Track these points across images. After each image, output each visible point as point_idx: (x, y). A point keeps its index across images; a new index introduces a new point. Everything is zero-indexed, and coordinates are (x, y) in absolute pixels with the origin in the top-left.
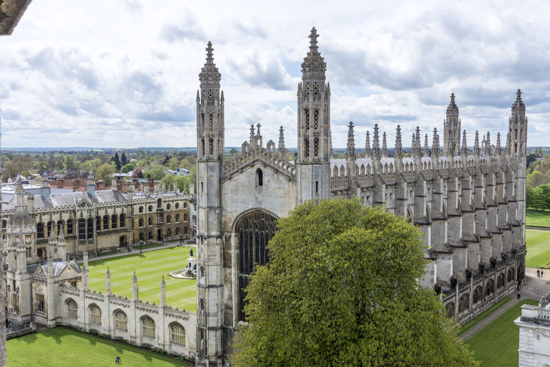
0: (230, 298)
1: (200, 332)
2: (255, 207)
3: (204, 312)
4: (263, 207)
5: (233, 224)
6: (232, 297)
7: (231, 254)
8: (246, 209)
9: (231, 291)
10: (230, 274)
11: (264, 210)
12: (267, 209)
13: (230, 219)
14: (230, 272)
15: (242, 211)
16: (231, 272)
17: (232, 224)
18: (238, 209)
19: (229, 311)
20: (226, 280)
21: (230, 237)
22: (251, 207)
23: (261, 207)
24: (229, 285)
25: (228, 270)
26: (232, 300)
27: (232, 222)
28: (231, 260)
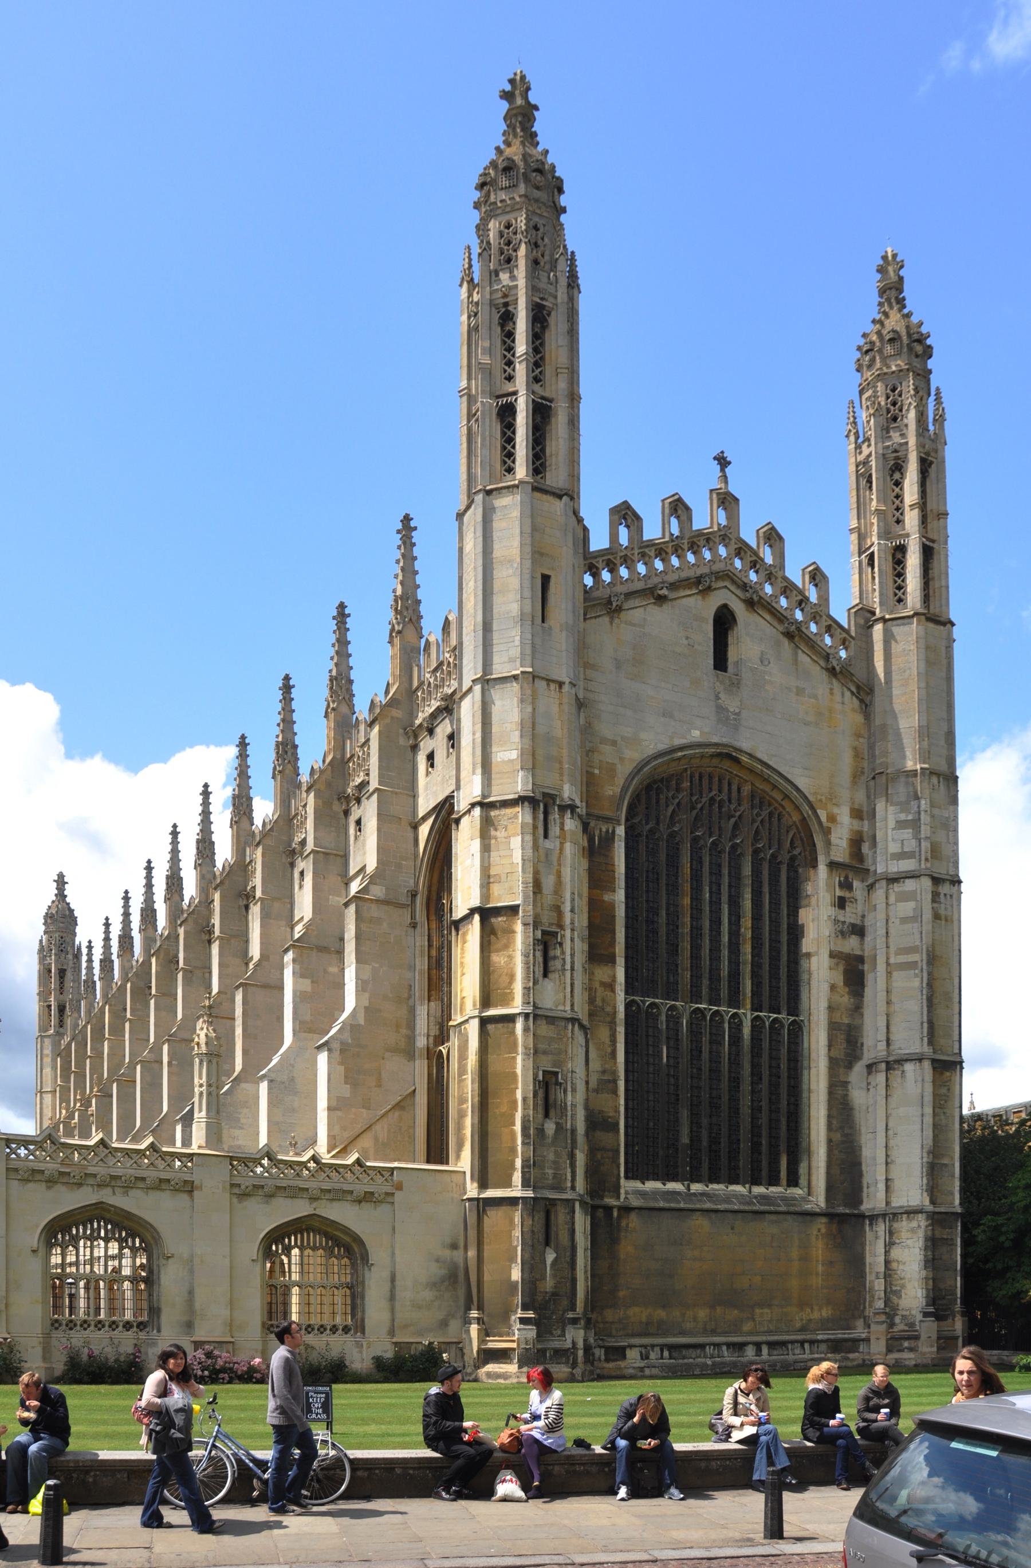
0: (608, 1084)
1: (540, 1216)
2: (715, 739)
3: (559, 1128)
4: (745, 745)
5: (625, 789)
6: (615, 1082)
7: (612, 906)
8: (678, 742)
9: (614, 1054)
10: (611, 986)
11: (750, 755)
12: (759, 755)
13: (611, 770)
14: (606, 979)
15: (662, 747)
16: (614, 978)
17: (618, 790)
18: (643, 735)
19: (604, 1138)
20: (599, 1011)
21: (609, 839)
22: (696, 735)
23: (737, 744)
24: (604, 1033)
25: (602, 973)
26: (615, 1092)
27: (620, 781)
28: (613, 932)
